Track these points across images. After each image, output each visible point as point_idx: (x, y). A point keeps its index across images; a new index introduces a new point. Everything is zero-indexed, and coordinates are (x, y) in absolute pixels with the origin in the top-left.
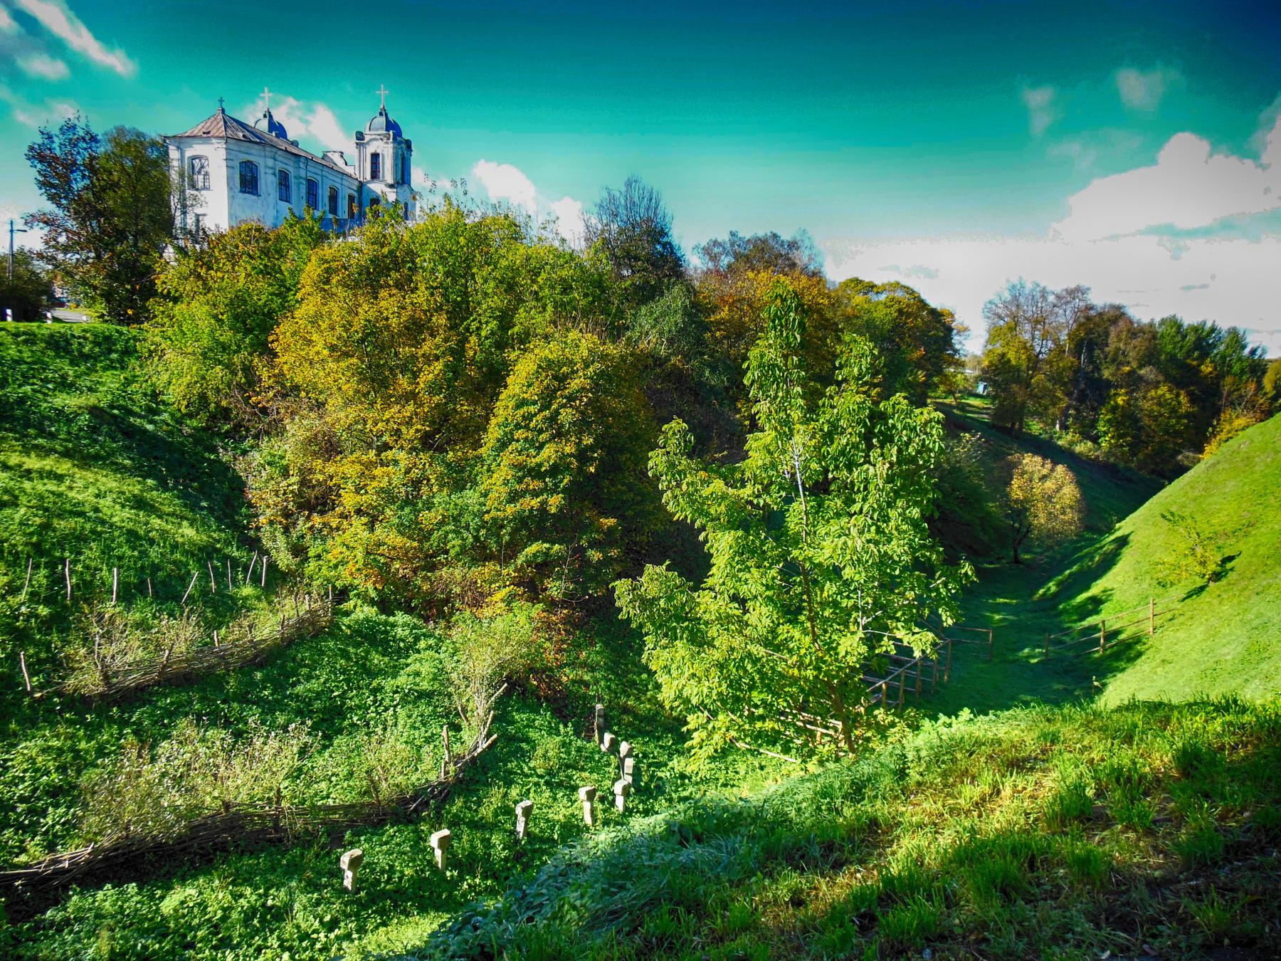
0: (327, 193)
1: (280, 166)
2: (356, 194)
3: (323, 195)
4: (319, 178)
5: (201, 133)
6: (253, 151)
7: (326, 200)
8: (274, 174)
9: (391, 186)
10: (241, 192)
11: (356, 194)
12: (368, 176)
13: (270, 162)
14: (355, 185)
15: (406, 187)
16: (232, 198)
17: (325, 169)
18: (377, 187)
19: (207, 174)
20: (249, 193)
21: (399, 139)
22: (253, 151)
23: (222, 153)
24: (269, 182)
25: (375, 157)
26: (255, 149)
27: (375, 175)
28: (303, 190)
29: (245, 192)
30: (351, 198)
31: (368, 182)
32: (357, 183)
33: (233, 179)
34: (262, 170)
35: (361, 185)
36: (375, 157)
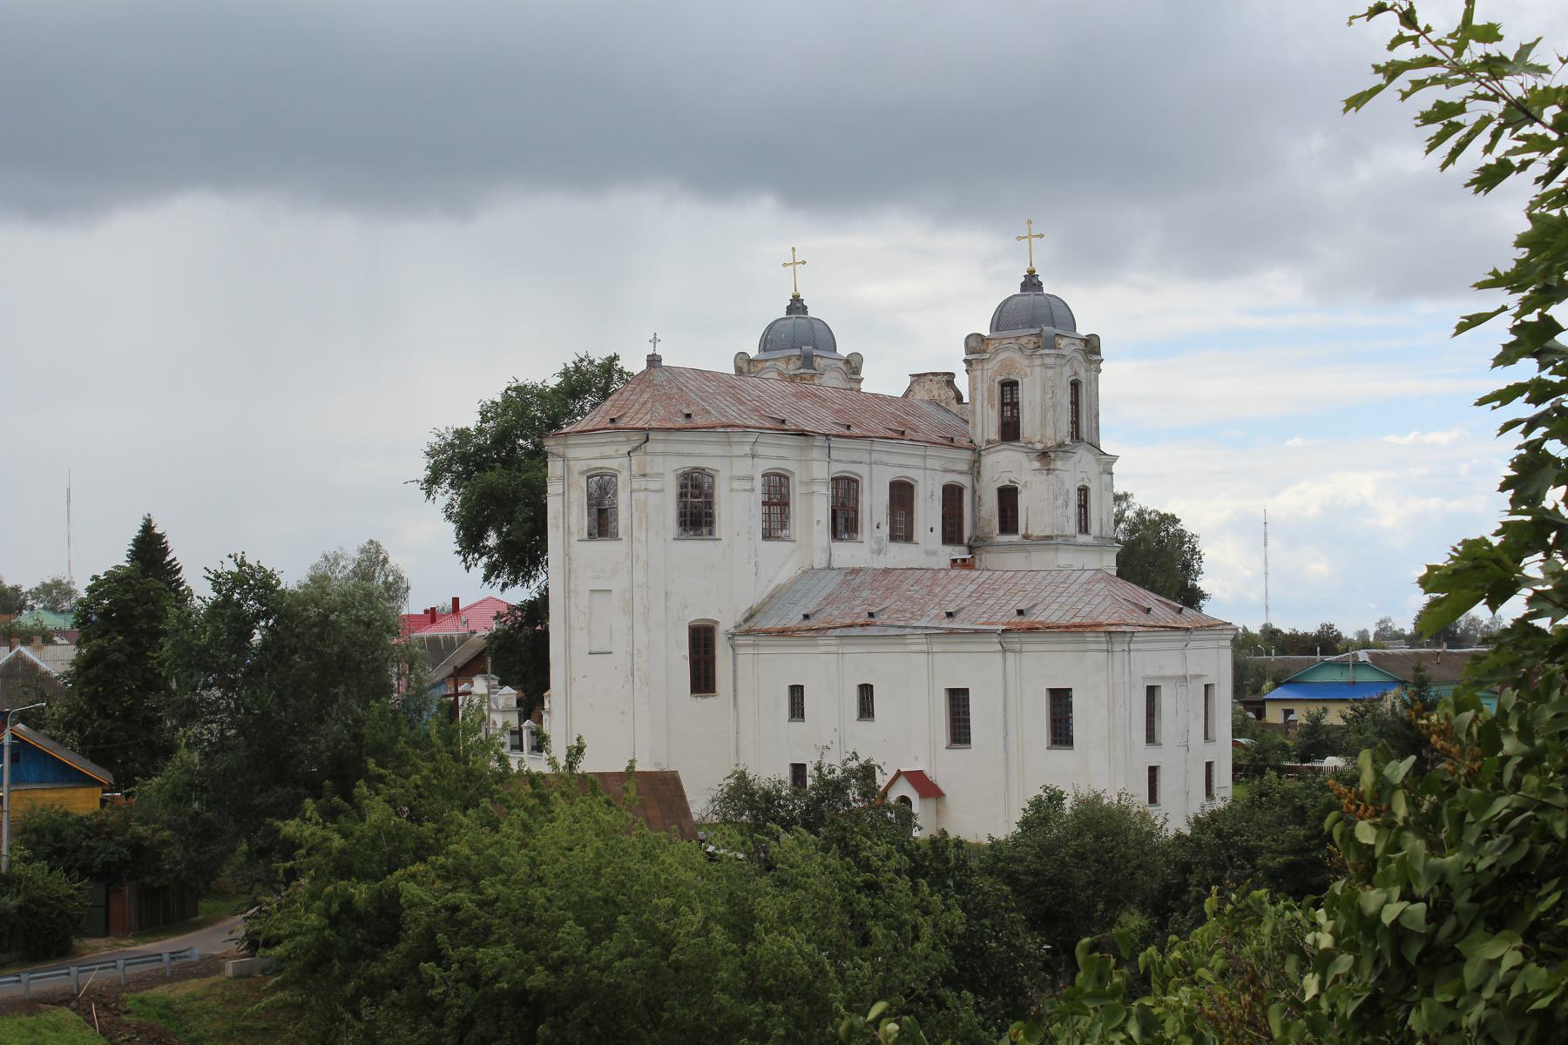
0: (884, 497)
1: (764, 465)
2: (965, 481)
3: (874, 504)
27: (1010, 431)
30: (952, 496)
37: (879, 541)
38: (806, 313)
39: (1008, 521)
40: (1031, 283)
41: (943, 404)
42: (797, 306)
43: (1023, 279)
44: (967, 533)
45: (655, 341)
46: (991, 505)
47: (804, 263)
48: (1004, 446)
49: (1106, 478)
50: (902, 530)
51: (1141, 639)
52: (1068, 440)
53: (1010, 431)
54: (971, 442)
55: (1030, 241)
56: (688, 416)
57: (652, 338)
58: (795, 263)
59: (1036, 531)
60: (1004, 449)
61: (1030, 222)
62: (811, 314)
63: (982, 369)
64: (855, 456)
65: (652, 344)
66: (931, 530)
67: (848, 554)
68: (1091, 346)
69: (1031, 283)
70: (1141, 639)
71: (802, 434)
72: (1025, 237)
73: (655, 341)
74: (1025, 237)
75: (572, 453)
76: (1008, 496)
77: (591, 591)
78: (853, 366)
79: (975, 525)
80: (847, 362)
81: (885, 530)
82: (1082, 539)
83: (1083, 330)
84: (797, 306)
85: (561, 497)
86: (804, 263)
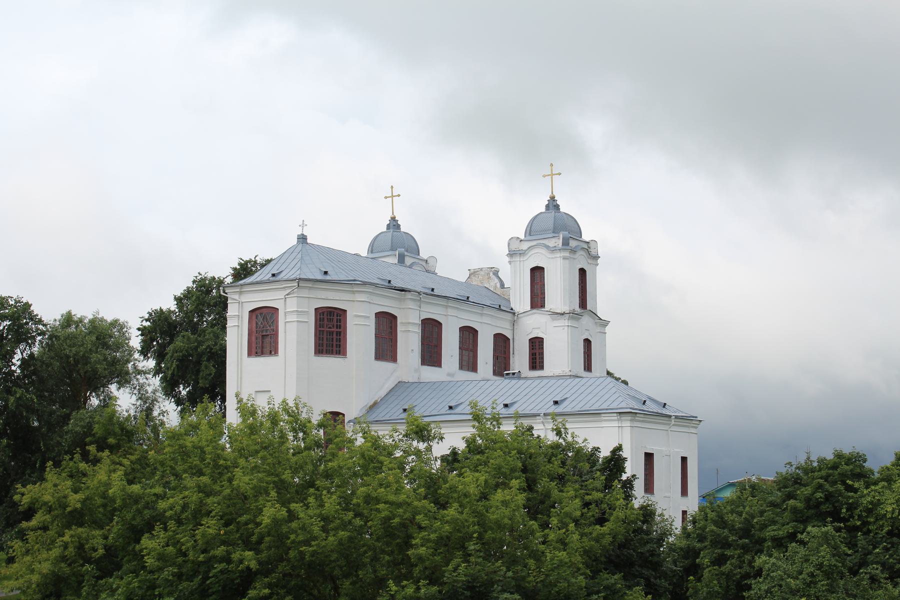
5: (266, 278)
25: (537, 273)
27: (538, 300)
36: (537, 273)
38: (400, 229)
39: (536, 360)
40: (553, 205)
41: (492, 289)
42: (394, 224)
43: (547, 203)
45: (303, 225)
47: (399, 196)
48: (534, 311)
50: (469, 362)
51: (641, 419)
52: (578, 309)
53: (538, 300)
54: (512, 309)
55: (552, 178)
56: (326, 273)
57: (301, 224)
58: (392, 196)
60: (535, 313)
61: (552, 165)
62: (403, 229)
63: (520, 261)
65: (301, 228)
66: (487, 363)
67: (430, 374)
69: (553, 205)
70: (641, 419)
71: (402, 290)
72: (549, 175)
73: (303, 225)
74: (549, 175)
75: (245, 298)
76: (536, 346)
77: (256, 392)
84: (394, 224)
85: (236, 327)
86: (399, 196)
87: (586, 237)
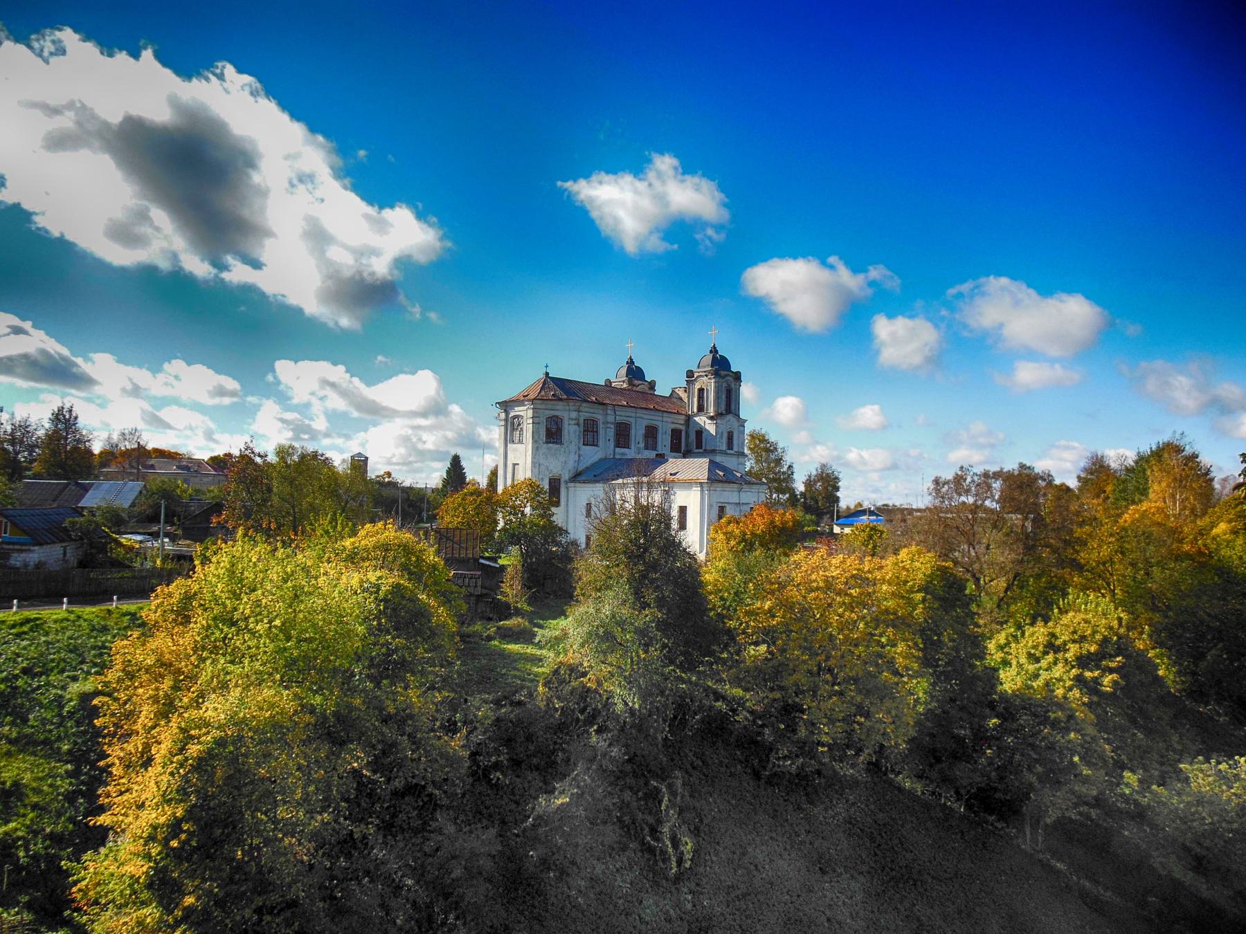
0: (642, 431)
1: (584, 416)
2: (683, 428)
3: (637, 433)
4: (632, 420)
6: (558, 407)
7: (641, 439)
8: (578, 424)
9: (711, 418)
10: (547, 442)
11: (683, 428)
12: (695, 410)
13: (574, 415)
14: (681, 419)
15: (730, 417)
16: (536, 449)
17: (639, 411)
18: (701, 420)
19: (522, 429)
20: (553, 443)
21: (723, 373)
22: (558, 407)
23: (530, 413)
24: (571, 431)
26: (560, 405)
27: (701, 409)
28: (611, 433)
29: (550, 442)
30: (676, 434)
31: (696, 415)
32: (683, 417)
33: (538, 432)
34: (566, 422)
35: (689, 418)
36: (701, 390)
37: (639, 449)
44: (683, 448)
46: (693, 437)
49: (742, 428)
59: (708, 448)
64: (627, 414)
68: (737, 377)
78: (652, 385)
79: (687, 445)
80: (650, 383)
81: (642, 445)
82: (729, 451)
83: (734, 369)
87: (734, 369)
